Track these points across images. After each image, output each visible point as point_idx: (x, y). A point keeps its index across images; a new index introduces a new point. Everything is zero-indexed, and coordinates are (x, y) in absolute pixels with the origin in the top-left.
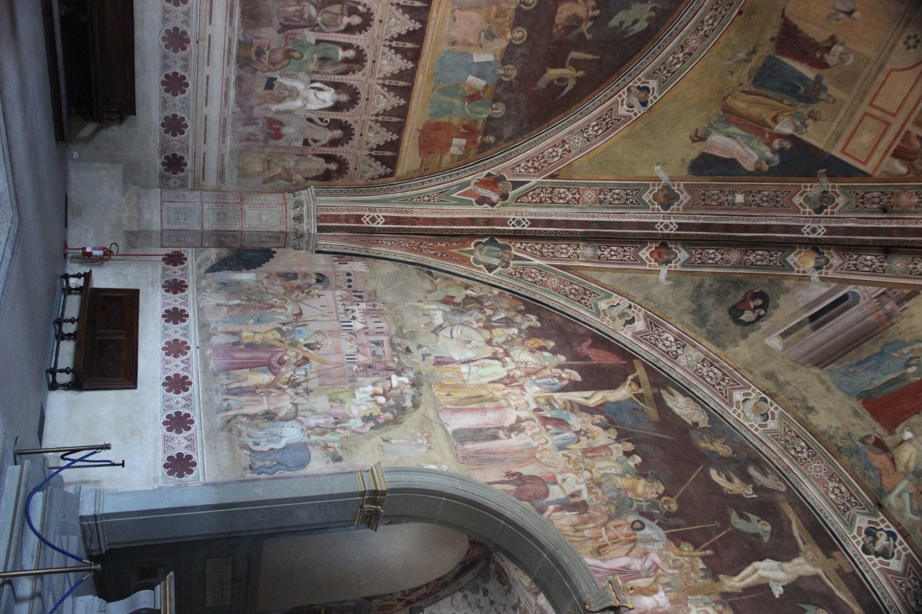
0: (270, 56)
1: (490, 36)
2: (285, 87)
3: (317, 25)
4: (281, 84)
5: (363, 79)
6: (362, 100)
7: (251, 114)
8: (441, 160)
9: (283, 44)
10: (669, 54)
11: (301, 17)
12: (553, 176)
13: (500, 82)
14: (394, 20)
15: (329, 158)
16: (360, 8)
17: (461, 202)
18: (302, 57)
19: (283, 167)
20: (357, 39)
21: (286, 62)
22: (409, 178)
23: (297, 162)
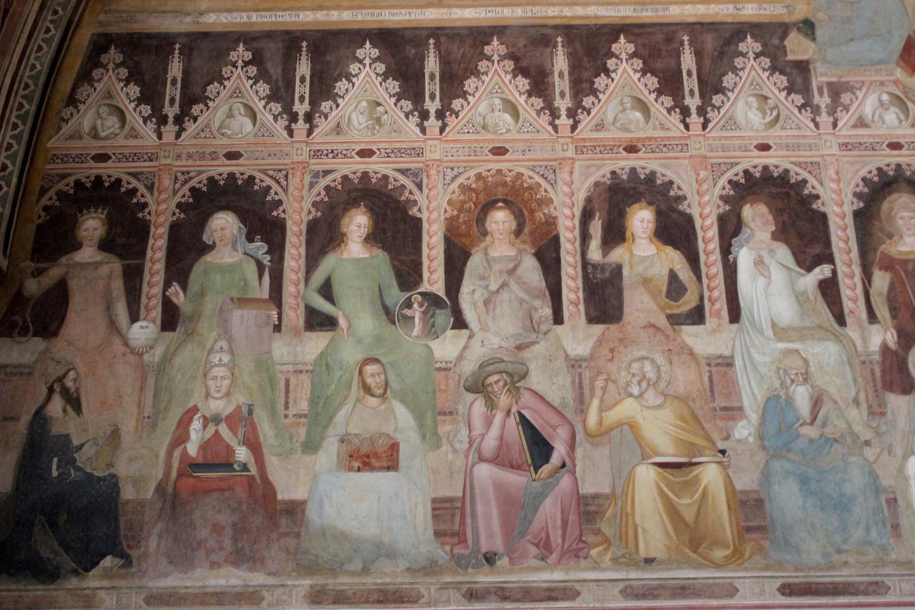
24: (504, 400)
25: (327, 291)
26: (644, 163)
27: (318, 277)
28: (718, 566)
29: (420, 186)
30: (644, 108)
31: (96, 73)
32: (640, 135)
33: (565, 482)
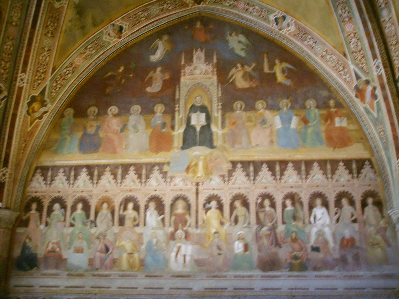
0: (298, 251)
1: (264, 122)
2: (317, 239)
3: (273, 225)
4: (315, 242)
5: (304, 192)
8: (354, 130)
10: (252, 16)
11: (269, 235)
12: (345, 55)
13: (292, 108)
14: (264, 180)
15: (364, 204)
16: (259, 201)
17: (379, 110)
20: (279, 201)
21: (299, 241)
22: (370, 149)
23: (371, 225)
24: (102, 241)
25: (74, 219)
26: (133, 194)
27: (73, 216)
28: (136, 271)
29: (91, 198)
30: (134, 182)
31: (36, 174)
32: (133, 187)
33: (111, 256)
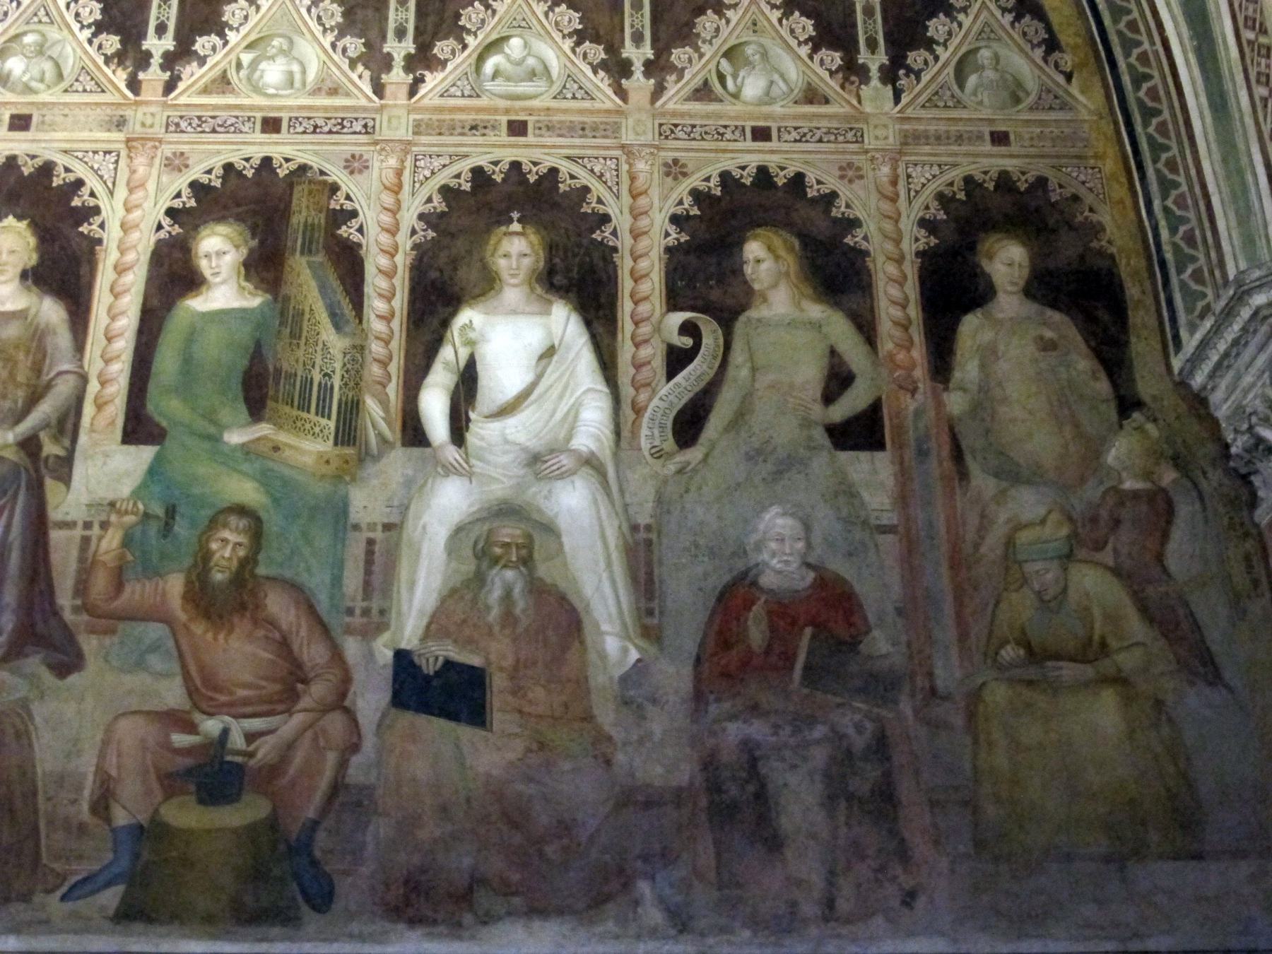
0: (238, 709)
3: (30, 445)
4: (436, 627)
5: (383, 166)
6: (523, 156)
7: (679, 797)
9: (155, 631)
18: (241, 510)
19: (1068, 557)
21: (277, 605)
